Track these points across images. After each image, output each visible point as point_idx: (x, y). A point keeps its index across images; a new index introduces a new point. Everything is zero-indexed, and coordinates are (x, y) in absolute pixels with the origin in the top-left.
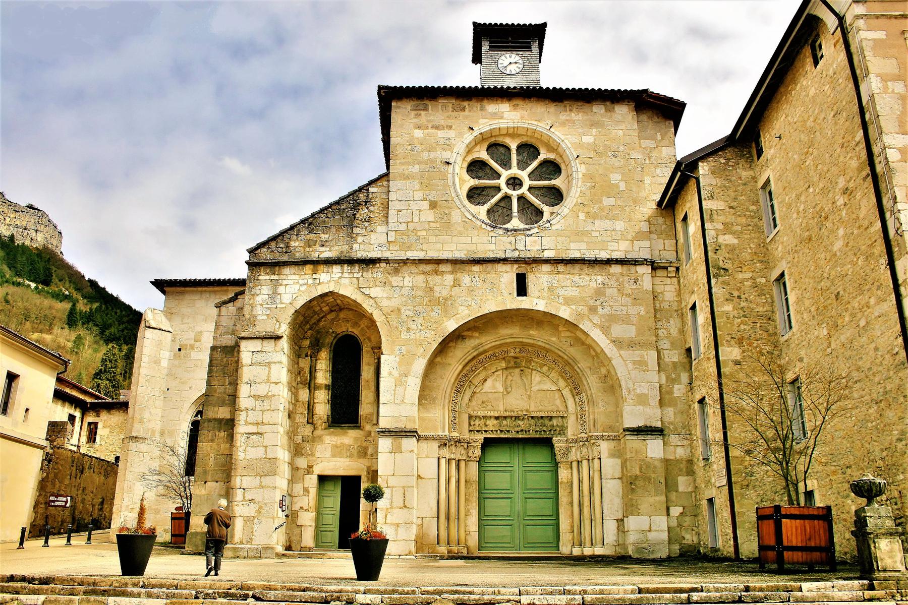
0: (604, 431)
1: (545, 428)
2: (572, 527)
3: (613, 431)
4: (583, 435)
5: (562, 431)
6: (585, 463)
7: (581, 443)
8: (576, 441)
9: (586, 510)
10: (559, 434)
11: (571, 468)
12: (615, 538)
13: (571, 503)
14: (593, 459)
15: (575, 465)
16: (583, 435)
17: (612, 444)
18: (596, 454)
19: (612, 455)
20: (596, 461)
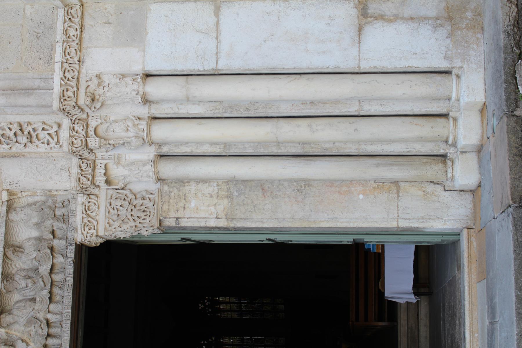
0: (51, 58)
1: (45, 269)
2: (380, 185)
3: (52, 28)
4: (65, 134)
5: (54, 210)
6: (161, 132)
7: (93, 142)
8: (84, 154)
9: (326, 134)
10: (65, 219)
11: (182, 182)
12: (426, 30)
13: (302, 186)
14: (146, 101)
15: (168, 169)
16: (65, 134)
17: (97, 31)
18: (130, 88)
19: (134, 33)
20: (156, 89)
